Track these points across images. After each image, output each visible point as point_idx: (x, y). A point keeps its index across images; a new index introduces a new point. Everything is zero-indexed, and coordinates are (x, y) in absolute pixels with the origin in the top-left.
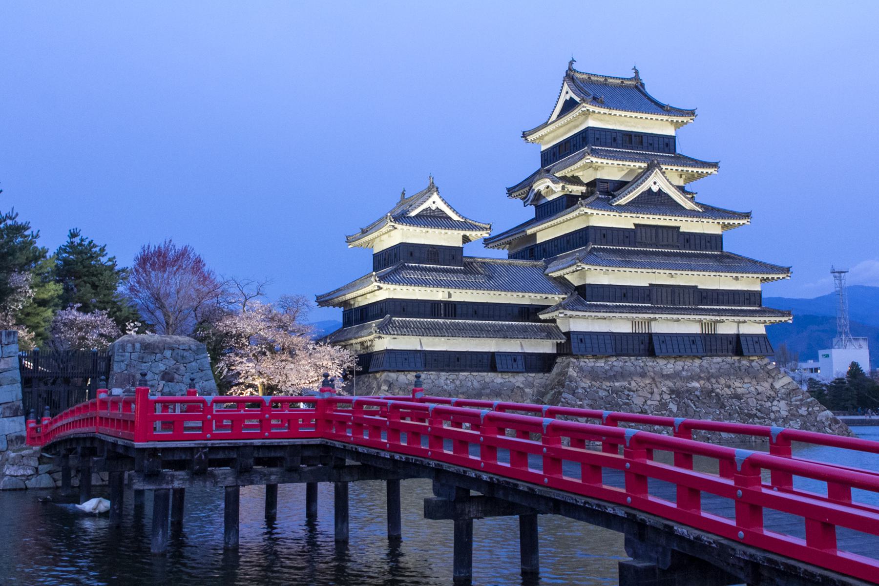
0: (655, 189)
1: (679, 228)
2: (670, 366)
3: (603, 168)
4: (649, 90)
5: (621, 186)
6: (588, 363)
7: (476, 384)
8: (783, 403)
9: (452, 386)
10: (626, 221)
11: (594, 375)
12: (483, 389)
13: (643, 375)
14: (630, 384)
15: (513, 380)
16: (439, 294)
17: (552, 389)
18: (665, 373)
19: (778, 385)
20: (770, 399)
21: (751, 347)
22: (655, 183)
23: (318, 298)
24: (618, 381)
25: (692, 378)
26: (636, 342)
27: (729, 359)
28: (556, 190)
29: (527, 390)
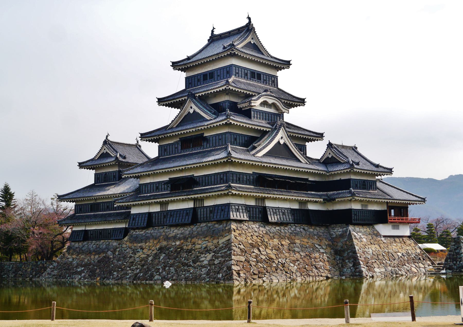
6: (138, 232)
12: (105, 249)
25: (180, 239)
26: (162, 217)
27: (209, 225)
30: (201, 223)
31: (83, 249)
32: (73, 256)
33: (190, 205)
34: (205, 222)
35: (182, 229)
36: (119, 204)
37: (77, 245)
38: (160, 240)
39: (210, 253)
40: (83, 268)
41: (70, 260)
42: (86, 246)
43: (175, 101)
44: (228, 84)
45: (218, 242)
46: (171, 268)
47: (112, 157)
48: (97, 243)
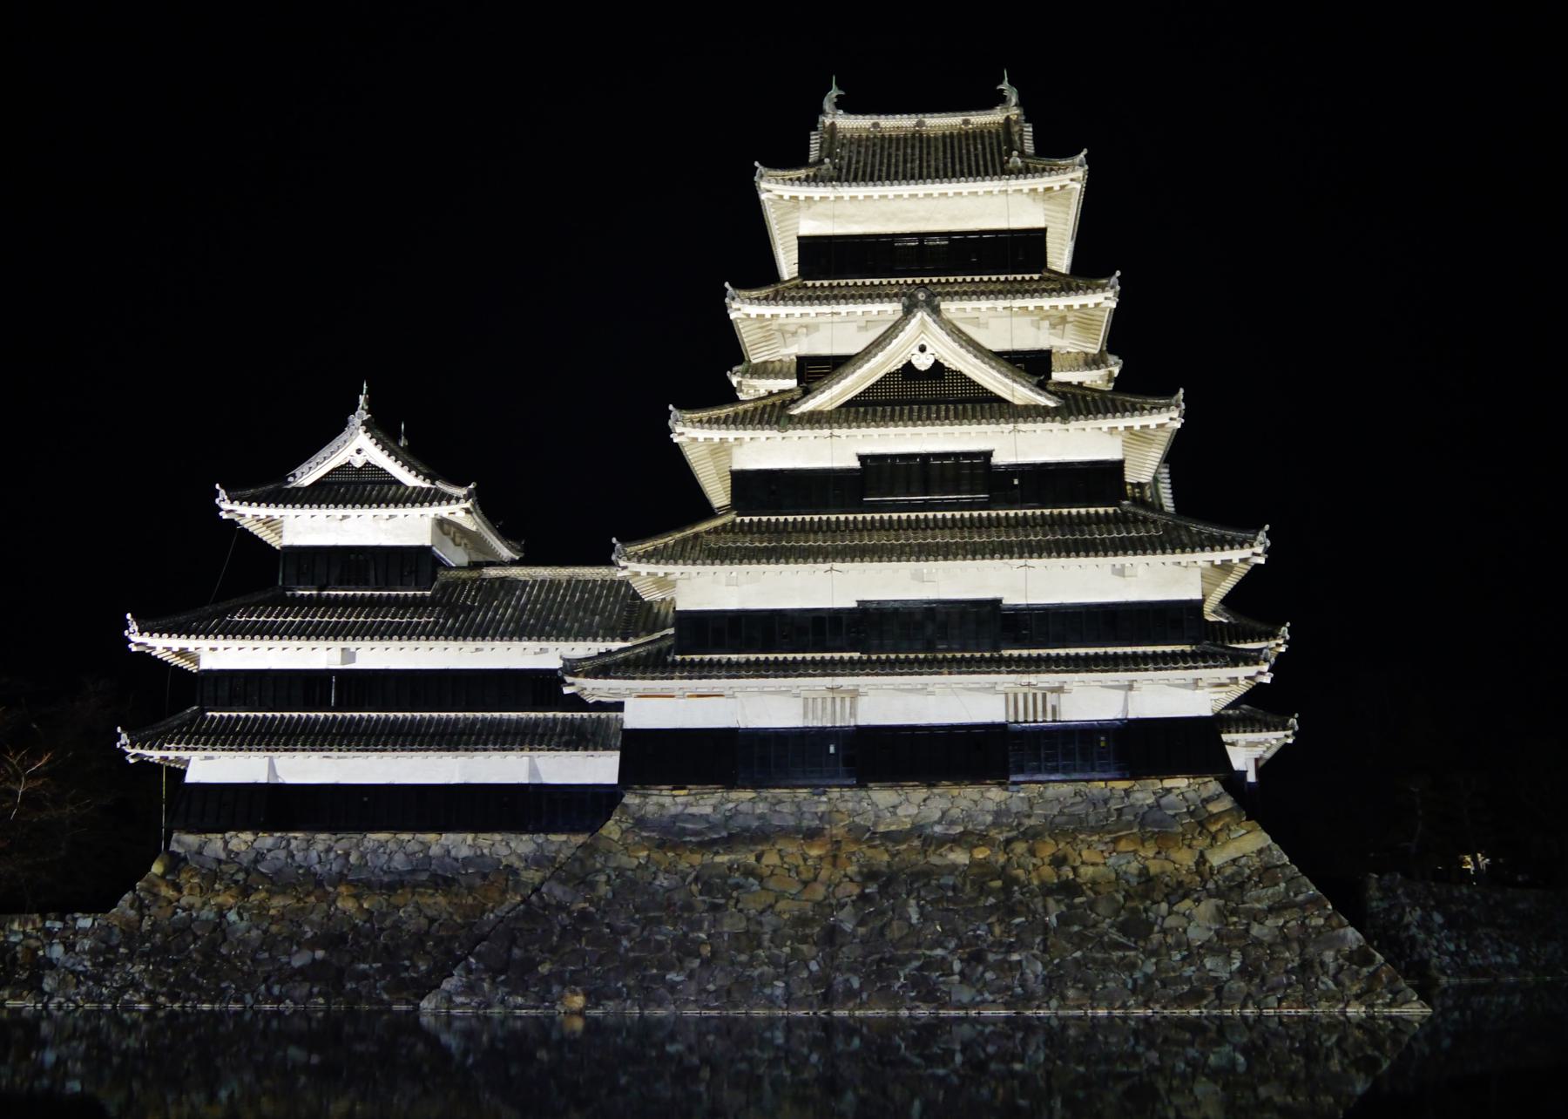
0: (923, 363)
1: (988, 455)
3: (816, 327)
5: (836, 365)
8: (1207, 908)
9: (335, 868)
10: (837, 451)
11: (670, 835)
12: (413, 872)
13: (812, 835)
14: (759, 858)
16: (319, 655)
18: (882, 829)
19: (1217, 859)
20: (1179, 891)
22: (923, 349)
24: (729, 850)
32: (220, 899)
39: (1198, 901)
40: (320, 954)
41: (208, 914)
42: (282, 854)
45: (1202, 860)
46: (1015, 957)
48: (345, 844)
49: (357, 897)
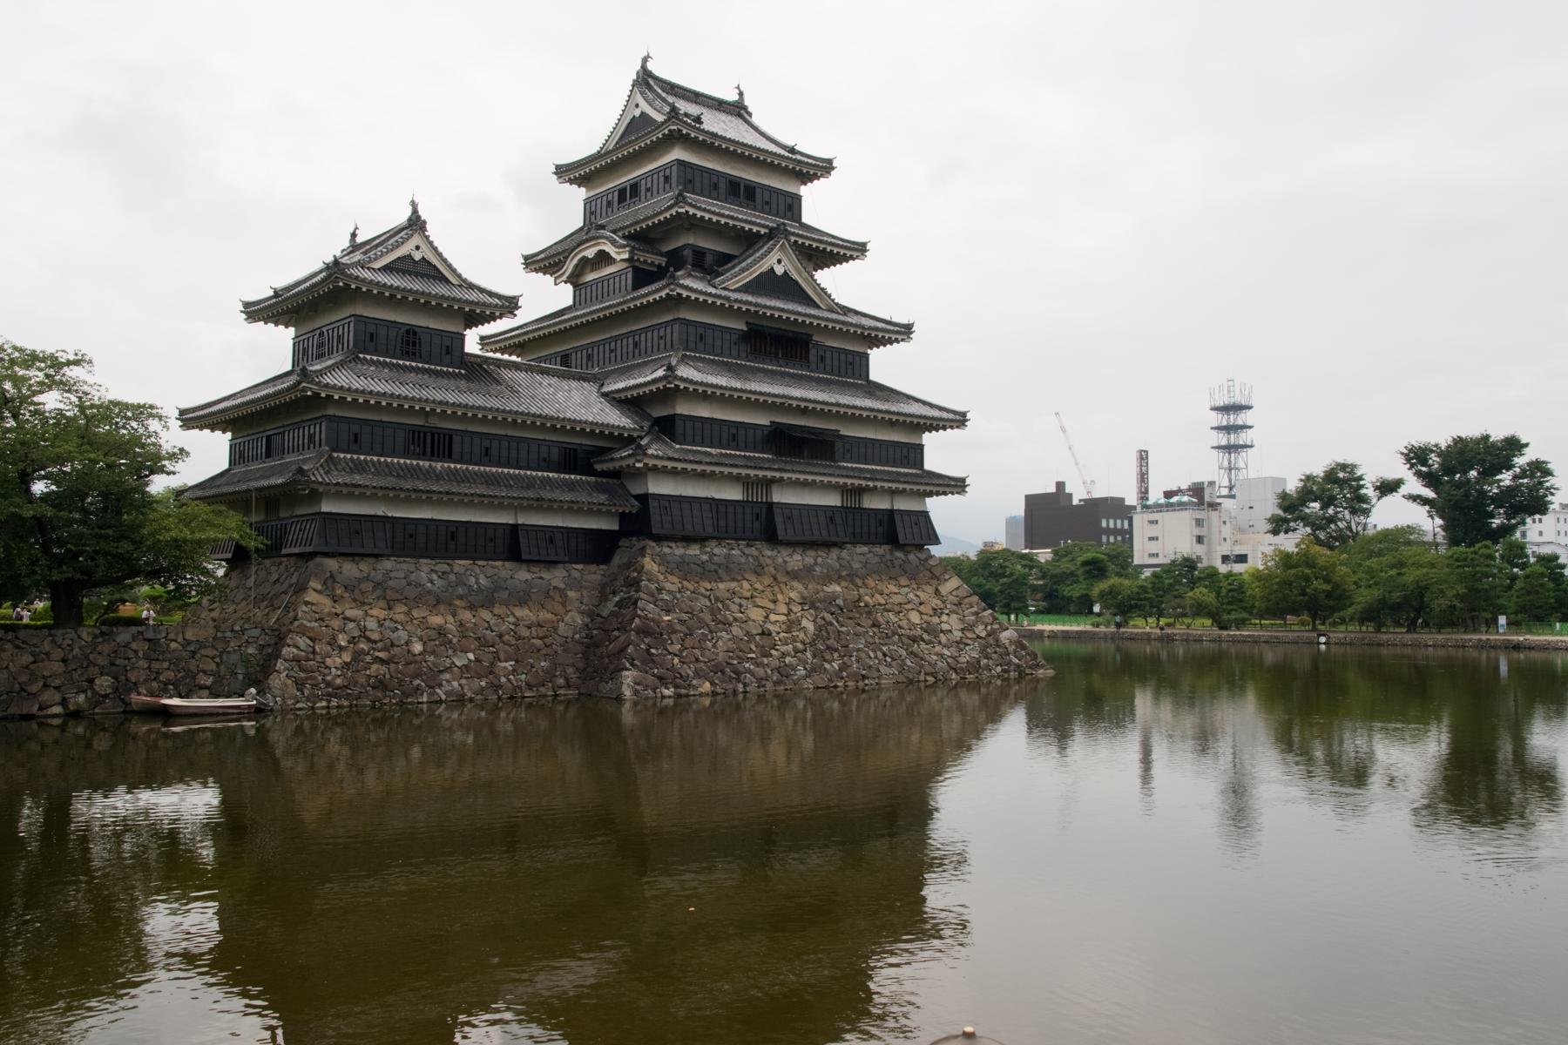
0: (779, 270)
2: (797, 557)
4: (755, 120)
6: (677, 551)
7: (482, 581)
8: (954, 616)
13: (759, 571)
15: (546, 575)
17: (614, 593)
20: (937, 612)
21: (908, 530)
22: (779, 261)
23: (182, 412)
25: (828, 579)
26: (748, 517)
28: (618, 258)
29: (571, 594)
30: (854, 543)
31: (391, 583)
32: (374, 612)
33: (833, 500)
34: (865, 544)
35: (813, 553)
36: (651, 462)
37: (350, 569)
38: (775, 579)
40: (471, 656)
43: (731, 222)
44: (696, 210)
45: (937, 592)
47: (447, 281)
49: (472, 607)
